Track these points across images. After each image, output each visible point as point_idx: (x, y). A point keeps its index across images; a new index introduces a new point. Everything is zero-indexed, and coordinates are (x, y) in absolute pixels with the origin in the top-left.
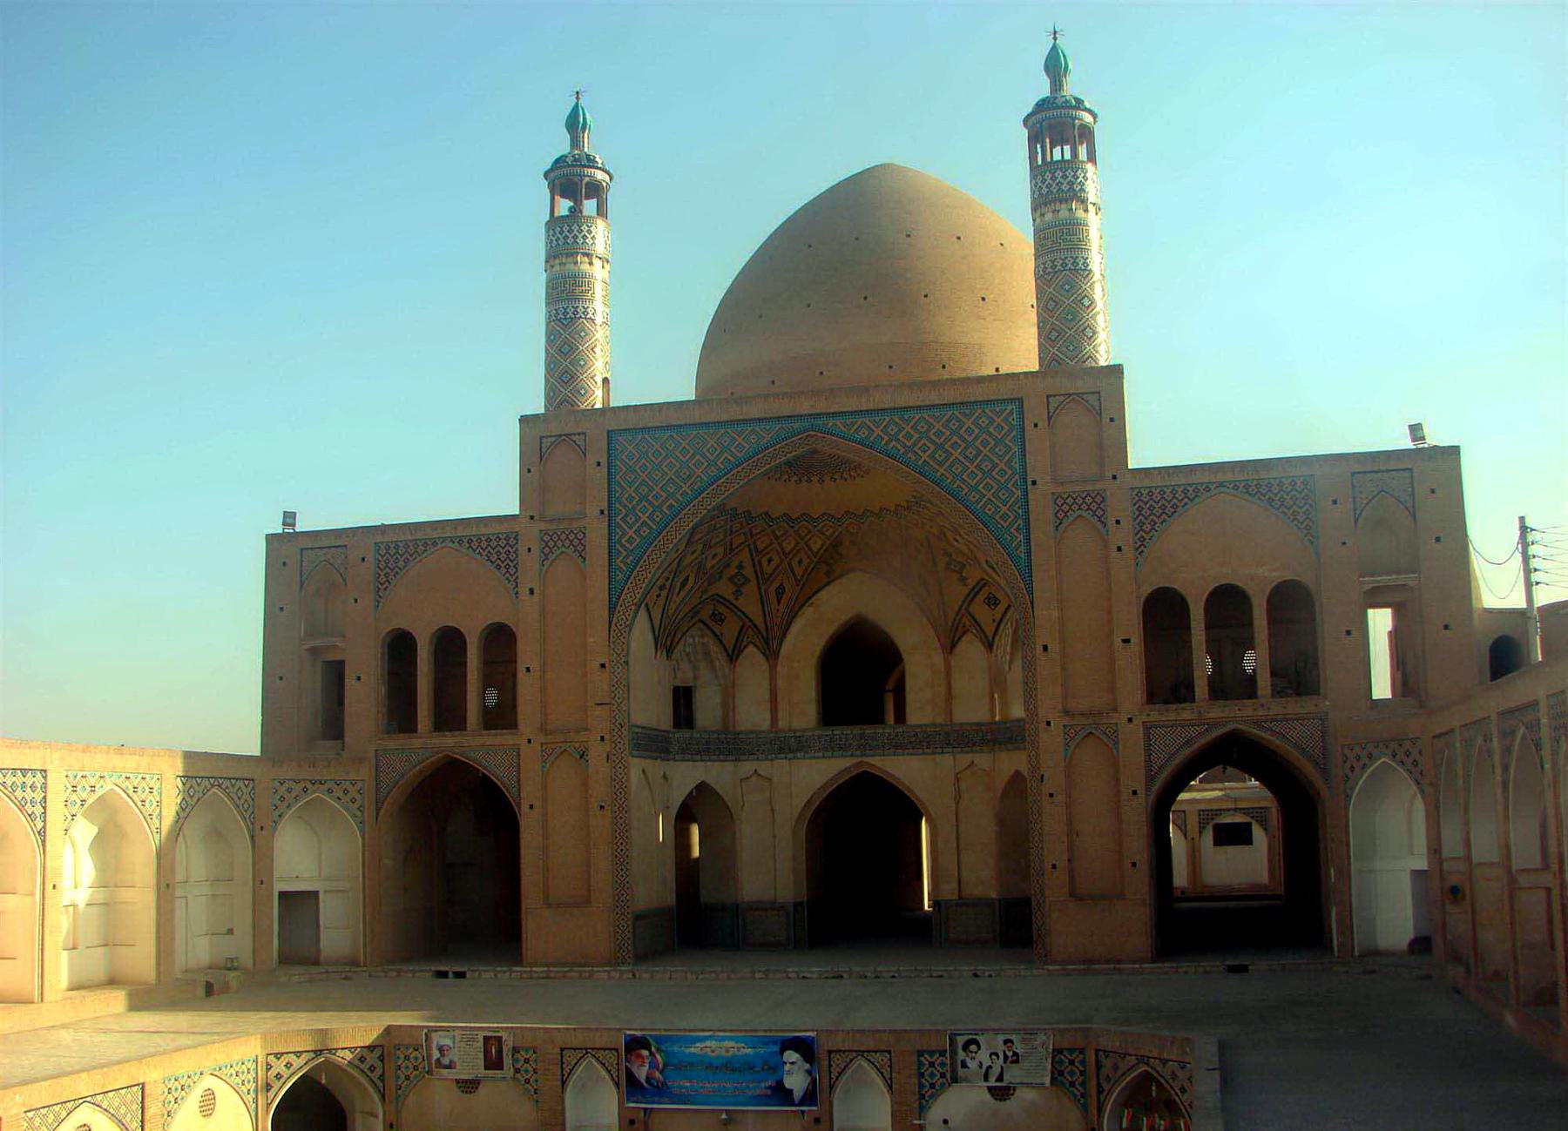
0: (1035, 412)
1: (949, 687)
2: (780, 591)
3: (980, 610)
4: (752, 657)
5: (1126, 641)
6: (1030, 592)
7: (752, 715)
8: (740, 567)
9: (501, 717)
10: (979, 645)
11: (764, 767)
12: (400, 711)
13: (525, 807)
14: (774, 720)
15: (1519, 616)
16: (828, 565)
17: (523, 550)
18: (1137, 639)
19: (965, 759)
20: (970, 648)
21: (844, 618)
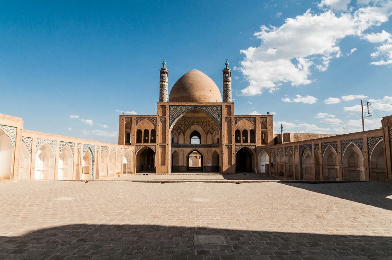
0: (223, 107)
1: (207, 140)
2: (186, 127)
3: (211, 130)
4: (181, 134)
5: (233, 136)
6: (222, 129)
7: (181, 142)
8: (182, 123)
9: (154, 141)
10: (210, 134)
11: (183, 149)
12: (139, 140)
13: (157, 153)
14: (184, 143)
15: (279, 135)
16: (193, 124)
17: (157, 120)
18: (235, 135)
19: (208, 148)
20: (209, 135)
21: (194, 130)
